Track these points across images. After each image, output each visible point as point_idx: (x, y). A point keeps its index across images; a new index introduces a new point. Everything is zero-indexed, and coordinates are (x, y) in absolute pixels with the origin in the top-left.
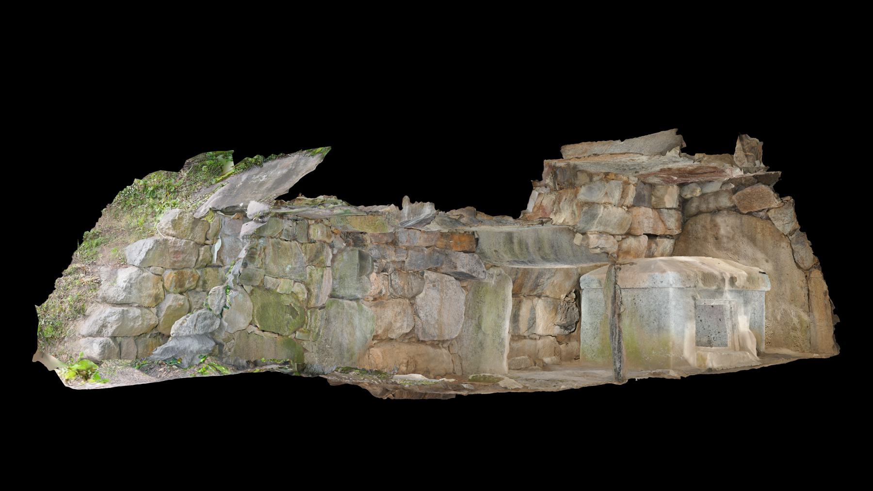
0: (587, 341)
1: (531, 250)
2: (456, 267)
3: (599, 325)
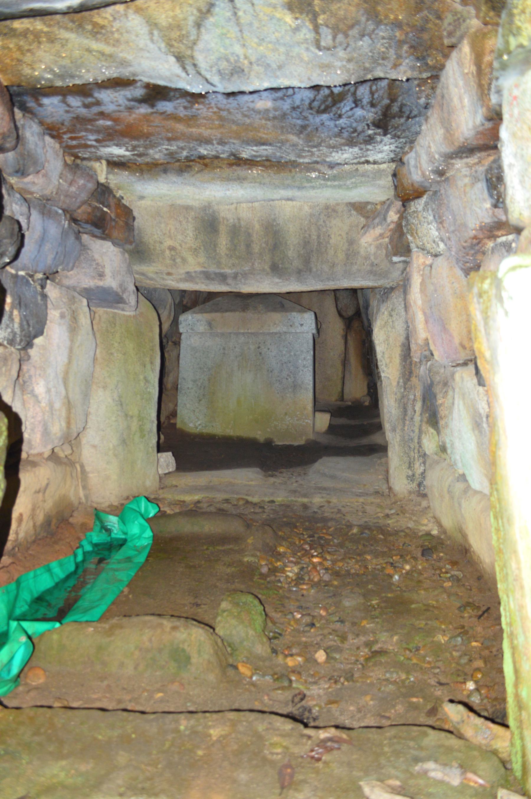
0: (188, 406)
1: (256, 248)
2: (101, 275)
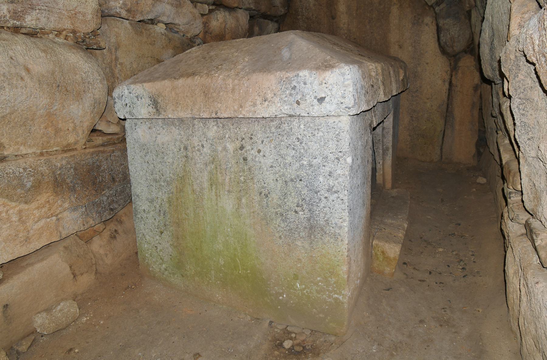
0: (147, 237)
3: (167, 205)
